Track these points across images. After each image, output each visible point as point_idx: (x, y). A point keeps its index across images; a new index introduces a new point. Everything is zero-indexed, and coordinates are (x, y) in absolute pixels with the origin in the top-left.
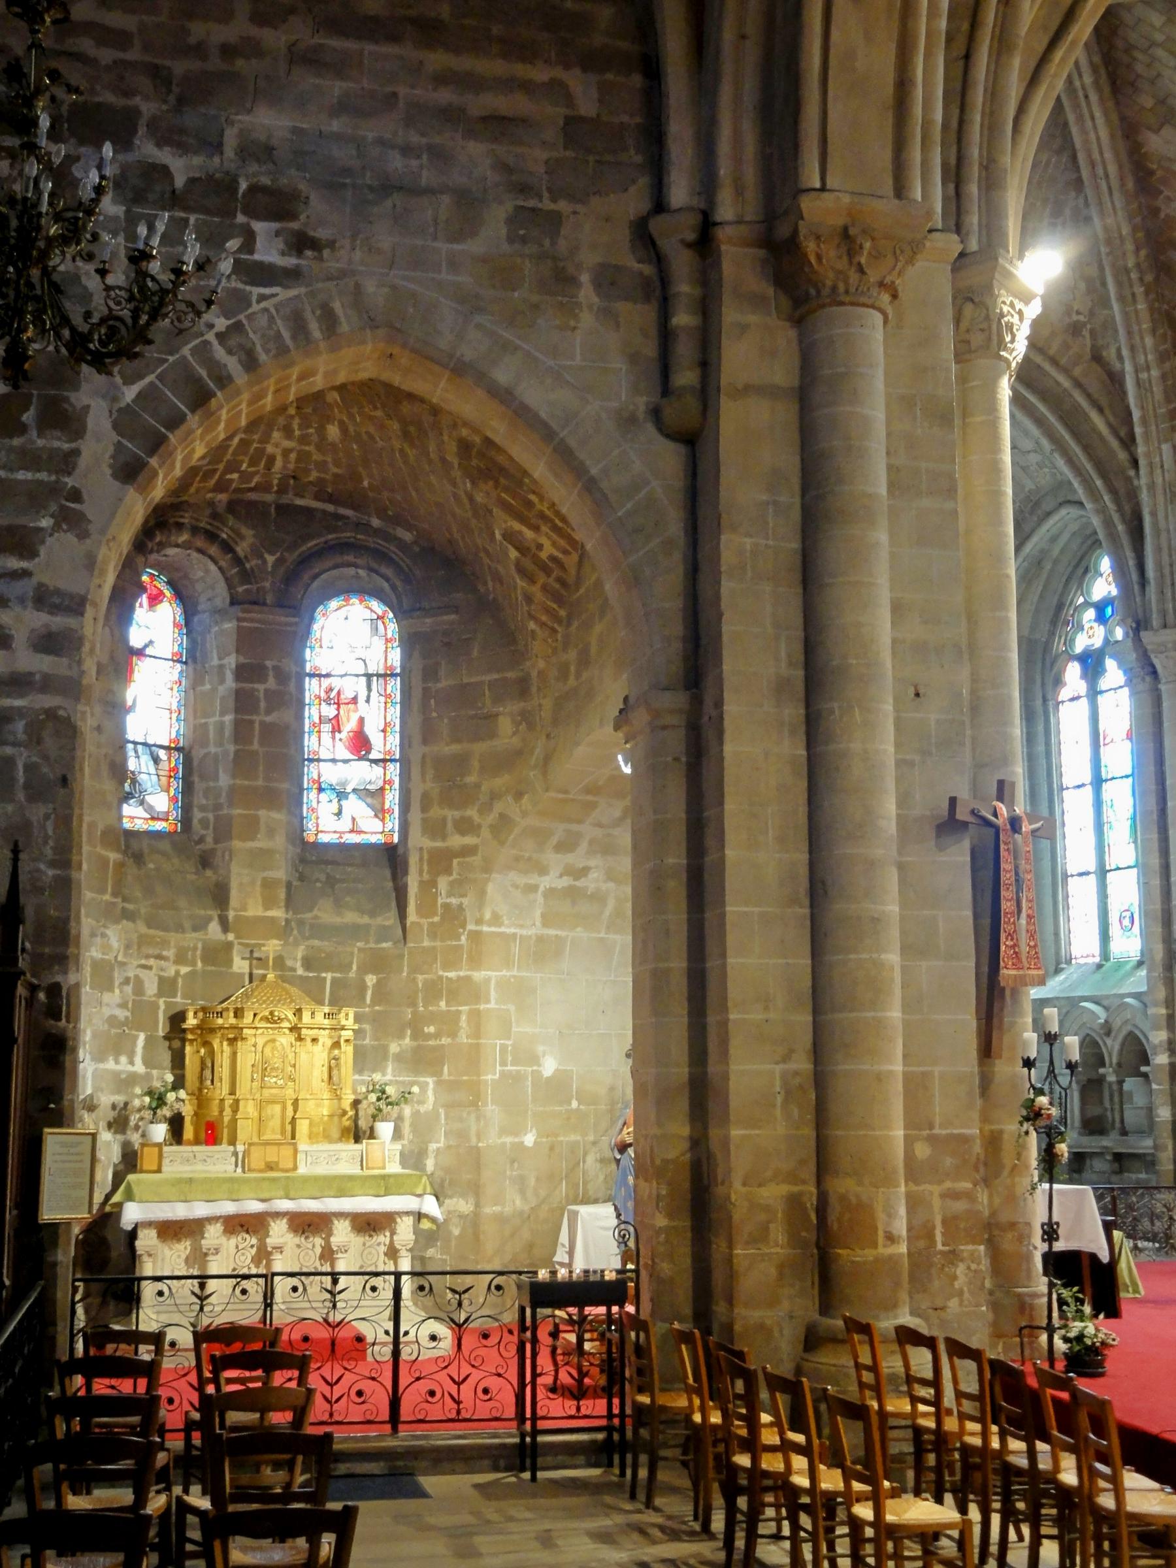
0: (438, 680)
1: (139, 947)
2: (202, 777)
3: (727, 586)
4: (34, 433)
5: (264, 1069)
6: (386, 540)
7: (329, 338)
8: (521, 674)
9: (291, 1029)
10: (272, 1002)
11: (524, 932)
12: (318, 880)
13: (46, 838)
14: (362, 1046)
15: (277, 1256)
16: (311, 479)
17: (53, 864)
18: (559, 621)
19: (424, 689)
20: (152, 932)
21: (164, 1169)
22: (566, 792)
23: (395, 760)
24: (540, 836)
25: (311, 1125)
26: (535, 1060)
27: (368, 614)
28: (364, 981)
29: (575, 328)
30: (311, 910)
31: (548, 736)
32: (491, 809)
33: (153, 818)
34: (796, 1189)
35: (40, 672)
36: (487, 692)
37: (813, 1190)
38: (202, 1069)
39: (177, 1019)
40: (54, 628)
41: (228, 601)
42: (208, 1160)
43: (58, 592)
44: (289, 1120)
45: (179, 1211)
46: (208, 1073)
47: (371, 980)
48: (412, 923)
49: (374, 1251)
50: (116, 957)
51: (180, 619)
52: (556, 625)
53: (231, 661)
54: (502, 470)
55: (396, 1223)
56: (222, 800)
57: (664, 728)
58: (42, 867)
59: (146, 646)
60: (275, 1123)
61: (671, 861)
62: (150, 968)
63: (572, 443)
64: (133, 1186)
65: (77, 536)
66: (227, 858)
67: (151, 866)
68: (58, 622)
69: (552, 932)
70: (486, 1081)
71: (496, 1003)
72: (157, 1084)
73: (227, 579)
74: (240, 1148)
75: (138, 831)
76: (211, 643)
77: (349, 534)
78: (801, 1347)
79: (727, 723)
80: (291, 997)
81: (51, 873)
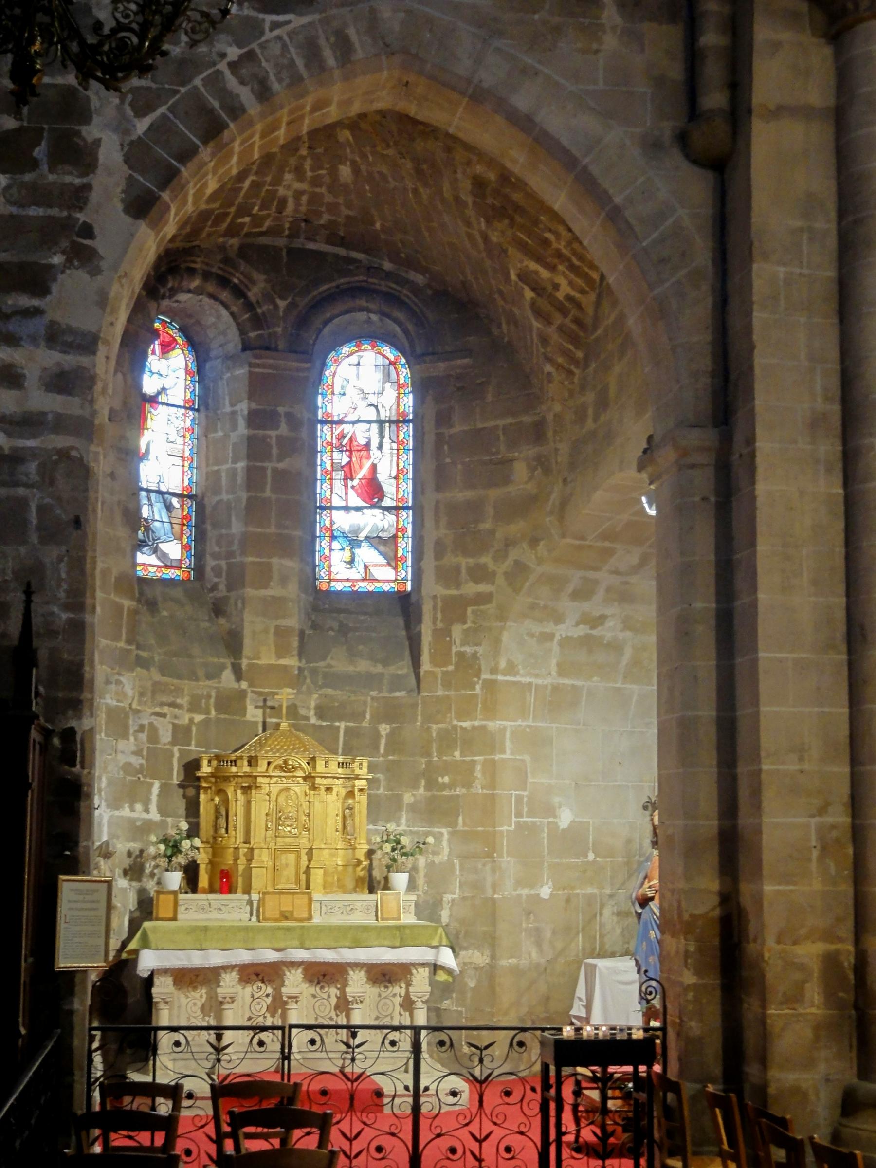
0: (452, 426)
2: (215, 525)
3: (759, 317)
4: (45, 168)
5: (278, 818)
6: (397, 283)
7: (342, 66)
8: (536, 418)
9: (305, 778)
10: (286, 751)
11: (540, 682)
12: (331, 629)
13: (60, 580)
14: (377, 795)
15: (292, 1005)
16: (322, 222)
17: (67, 607)
18: (576, 362)
19: (437, 434)
20: (165, 679)
21: (180, 916)
22: (583, 538)
23: (408, 508)
24: (557, 584)
25: (325, 874)
26: (550, 811)
27: (380, 360)
29: (597, 51)
30: (324, 658)
31: (565, 480)
32: (506, 556)
33: (166, 566)
34: (833, 947)
35: (52, 412)
36: (502, 438)
37: (851, 948)
38: (217, 818)
39: (191, 767)
40: (66, 367)
41: (240, 347)
42: (223, 908)
43: (70, 330)
44: (303, 869)
45: (196, 959)
46: (222, 822)
47: (384, 729)
48: (426, 671)
49: (389, 1003)
50: (130, 704)
51: (192, 366)
52: (572, 367)
53: (243, 407)
54: (518, 209)
55: (411, 974)
56: (235, 547)
57: (693, 466)
58: (56, 609)
59: (159, 393)
60: (290, 872)
61: (699, 605)
62: (164, 716)
63: (595, 170)
64: (149, 933)
65: (89, 273)
66: (240, 605)
67: (165, 613)
68: (70, 360)
69: (567, 681)
70: (502, 832)
71: (512, 754)
72: (172, 832)
73: (238, 324)
74: (255, 897)
75: (152, 580)
76: (223, 390)
77: (361, 278)
78: (839, 1110)
79: (759, 460)
80: (304, 746)
81: (64, 616)
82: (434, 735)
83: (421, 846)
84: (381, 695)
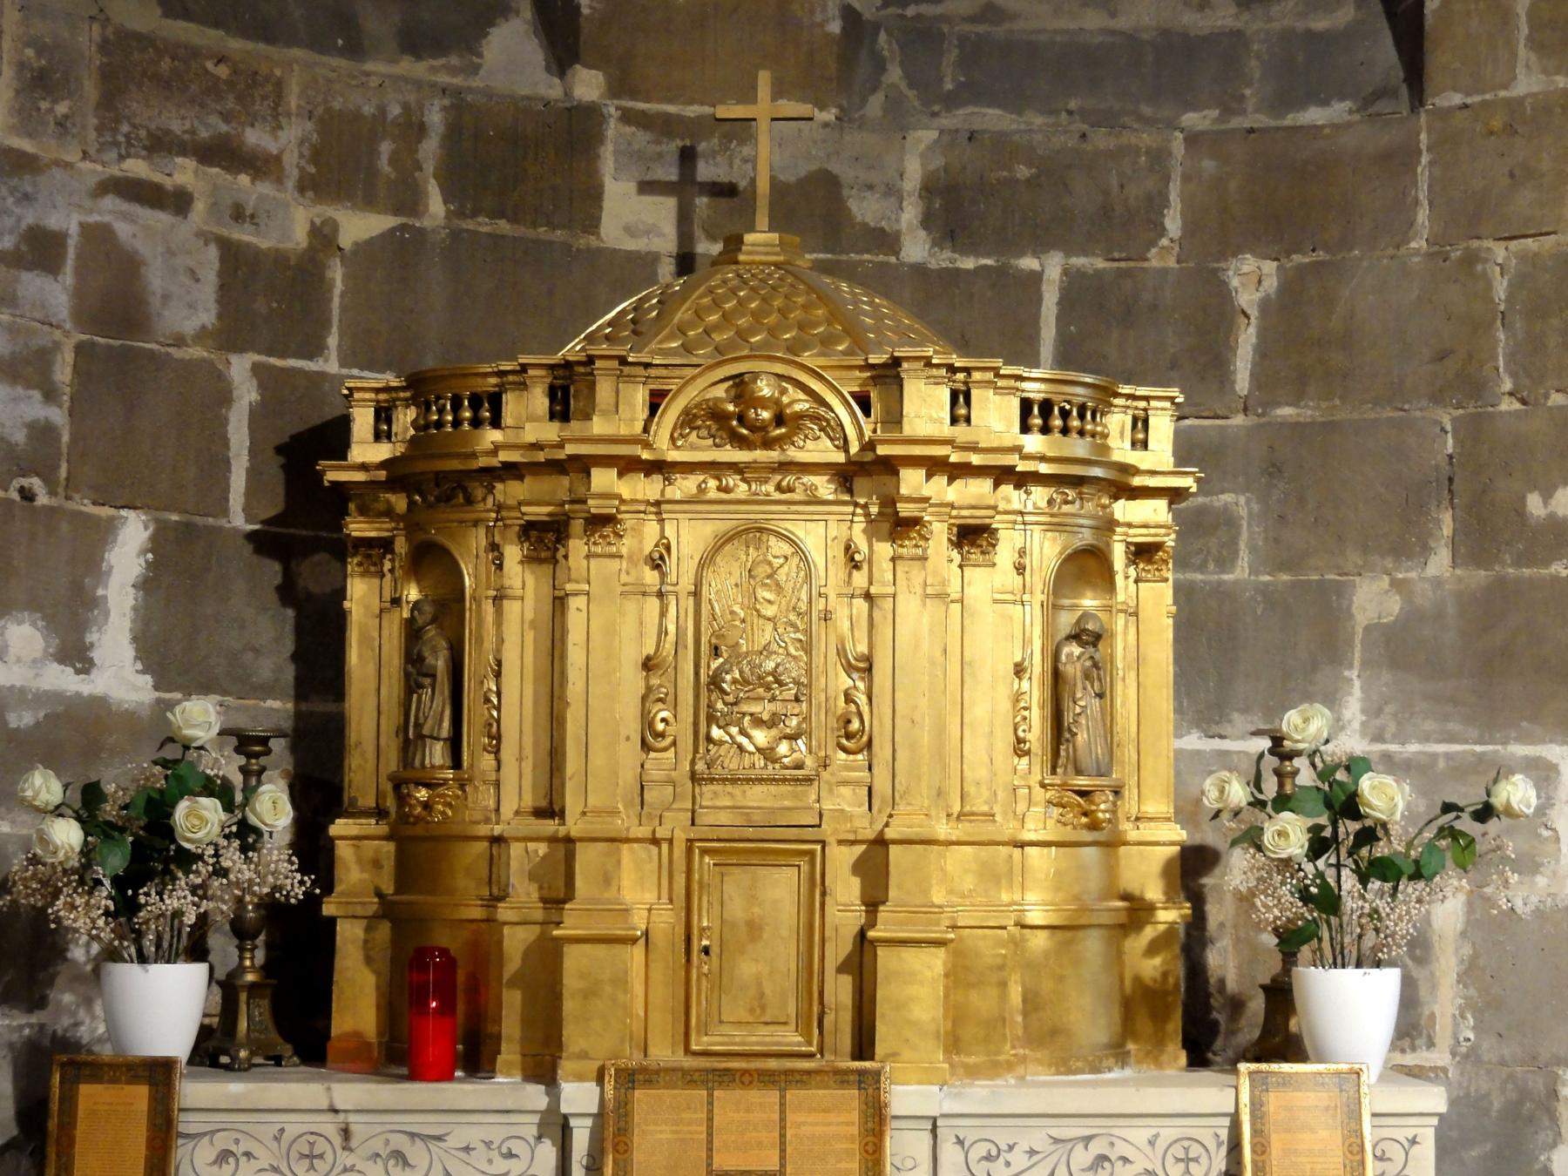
1: (109, 102)
9: (846, 476)
14: (1222, 593)
25: (960, 975)
28: (1223, 293)
38: (411, 686)
42: (415, 1152)
44: (840, 948)
62: (180, 202)
82: (1501, 289)
83: (1466, 824)
84: (1236, 122)
